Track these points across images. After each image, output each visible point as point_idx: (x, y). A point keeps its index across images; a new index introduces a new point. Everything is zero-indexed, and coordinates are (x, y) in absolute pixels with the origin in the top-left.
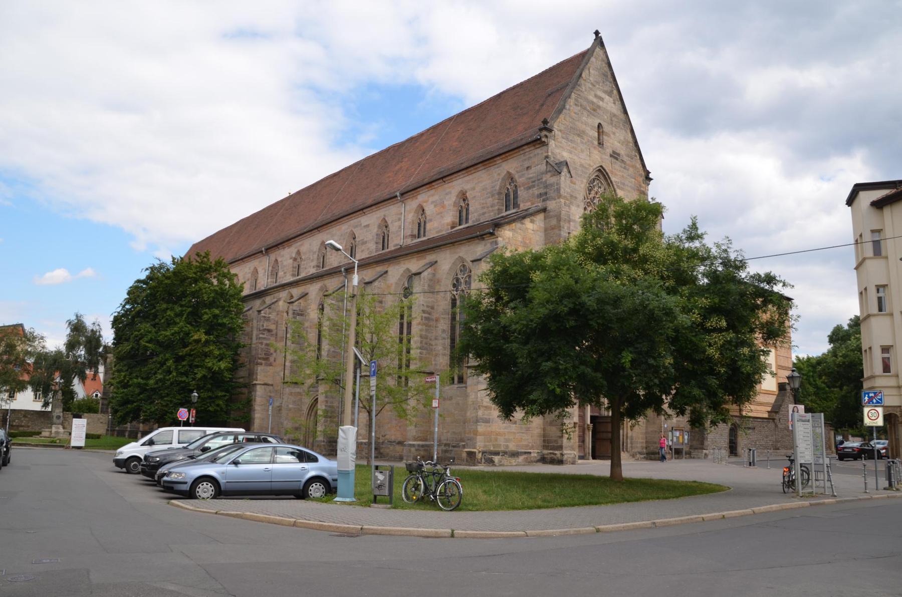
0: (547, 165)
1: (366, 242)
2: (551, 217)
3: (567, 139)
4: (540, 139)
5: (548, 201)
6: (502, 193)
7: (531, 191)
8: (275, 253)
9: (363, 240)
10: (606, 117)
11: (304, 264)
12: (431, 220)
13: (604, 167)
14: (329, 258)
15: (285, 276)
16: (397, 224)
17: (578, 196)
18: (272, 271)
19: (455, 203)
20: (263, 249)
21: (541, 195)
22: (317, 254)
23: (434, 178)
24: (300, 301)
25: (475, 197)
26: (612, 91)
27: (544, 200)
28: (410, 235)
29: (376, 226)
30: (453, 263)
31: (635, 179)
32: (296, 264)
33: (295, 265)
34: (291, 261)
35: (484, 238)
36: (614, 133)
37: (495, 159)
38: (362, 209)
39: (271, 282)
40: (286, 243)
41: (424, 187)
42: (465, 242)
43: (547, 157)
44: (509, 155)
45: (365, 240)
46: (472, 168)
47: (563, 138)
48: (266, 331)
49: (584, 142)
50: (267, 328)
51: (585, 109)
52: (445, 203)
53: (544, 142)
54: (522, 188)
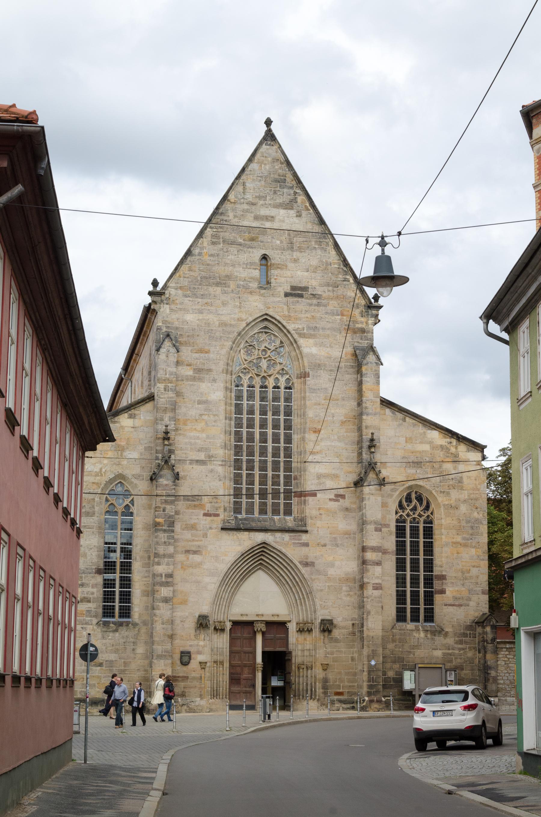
3: (195, 296)
10: (278, 242)
13: (271, 313)
17: (213, 367)
26: (295, 200)
31: (342, 315)
36: (296, 261)
47: (186, 296)
49: (230, 290)
51: (233, 243)
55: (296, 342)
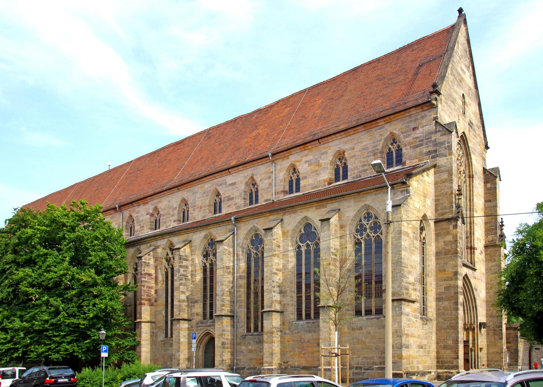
0: (436, 126)
1: (233, 198)
2: (442, 172)
4: (429, 102)
5: (438, 158)
6: (384, 152)
7: (418, 149)
8: (129, 209)
9: (229, 196)
11: (163, 219)
12: (305, 178)
14: (191, 213)
15: (142, 230)
16: (267, 182)
18: (126, 225)
19: (331, 161)
20: (117, 206)
21: (429, 152)
22: (177, 209)
23: (309, 139)
24: (185, 247)
25: (354, 156)
27: (433, 157)
28: (282, 191)
29: (243, 184)
30: (358, 211)
32: (153, 219)
33: (152, 221)
34: (148, 216)
35: (394, 187)
37: (378, 121)
38: (228, 169)
39: (126, 235)
40: (142, 201)
41: (298, 148)
42: (373, 191)
44: (394, 117)
45: (232, 196)
46: (352, 130)
48: (147, 275)
50: (148, 272)
52: (321, 162)
53: (434, 104)
54: (409, 147)
55: (470, 155)
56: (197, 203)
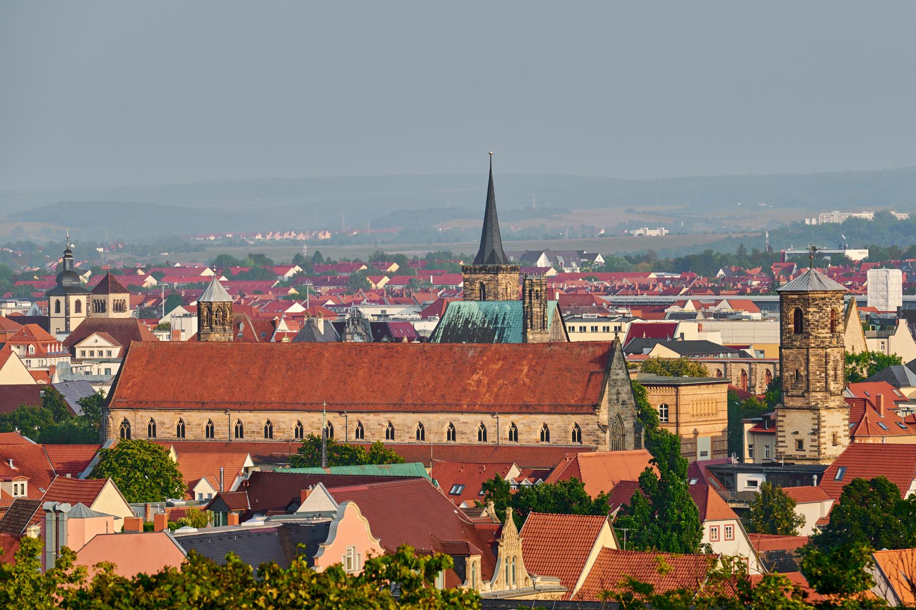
21: (595, 441)
43: (598, 422)
56: (432, 428)
